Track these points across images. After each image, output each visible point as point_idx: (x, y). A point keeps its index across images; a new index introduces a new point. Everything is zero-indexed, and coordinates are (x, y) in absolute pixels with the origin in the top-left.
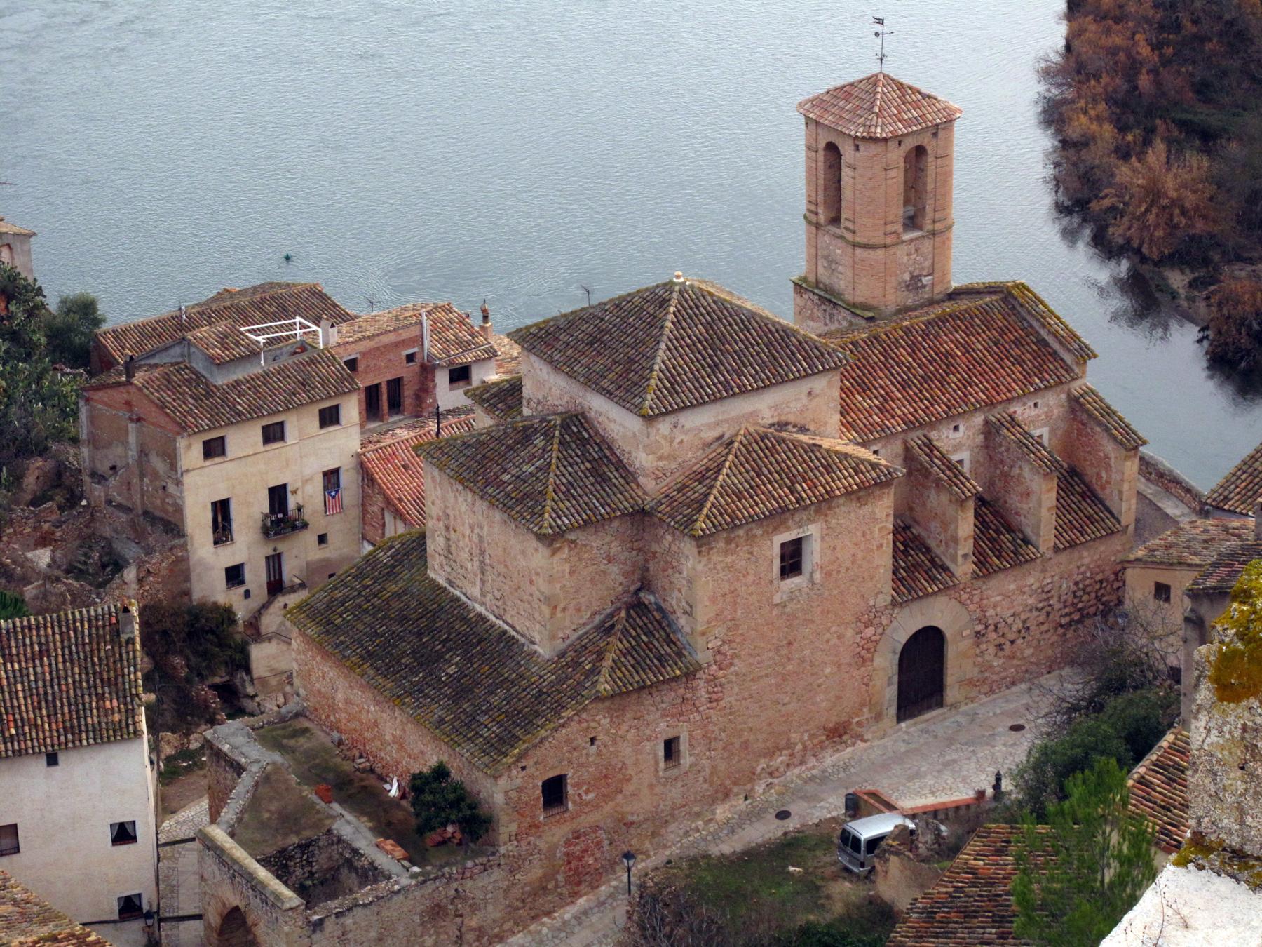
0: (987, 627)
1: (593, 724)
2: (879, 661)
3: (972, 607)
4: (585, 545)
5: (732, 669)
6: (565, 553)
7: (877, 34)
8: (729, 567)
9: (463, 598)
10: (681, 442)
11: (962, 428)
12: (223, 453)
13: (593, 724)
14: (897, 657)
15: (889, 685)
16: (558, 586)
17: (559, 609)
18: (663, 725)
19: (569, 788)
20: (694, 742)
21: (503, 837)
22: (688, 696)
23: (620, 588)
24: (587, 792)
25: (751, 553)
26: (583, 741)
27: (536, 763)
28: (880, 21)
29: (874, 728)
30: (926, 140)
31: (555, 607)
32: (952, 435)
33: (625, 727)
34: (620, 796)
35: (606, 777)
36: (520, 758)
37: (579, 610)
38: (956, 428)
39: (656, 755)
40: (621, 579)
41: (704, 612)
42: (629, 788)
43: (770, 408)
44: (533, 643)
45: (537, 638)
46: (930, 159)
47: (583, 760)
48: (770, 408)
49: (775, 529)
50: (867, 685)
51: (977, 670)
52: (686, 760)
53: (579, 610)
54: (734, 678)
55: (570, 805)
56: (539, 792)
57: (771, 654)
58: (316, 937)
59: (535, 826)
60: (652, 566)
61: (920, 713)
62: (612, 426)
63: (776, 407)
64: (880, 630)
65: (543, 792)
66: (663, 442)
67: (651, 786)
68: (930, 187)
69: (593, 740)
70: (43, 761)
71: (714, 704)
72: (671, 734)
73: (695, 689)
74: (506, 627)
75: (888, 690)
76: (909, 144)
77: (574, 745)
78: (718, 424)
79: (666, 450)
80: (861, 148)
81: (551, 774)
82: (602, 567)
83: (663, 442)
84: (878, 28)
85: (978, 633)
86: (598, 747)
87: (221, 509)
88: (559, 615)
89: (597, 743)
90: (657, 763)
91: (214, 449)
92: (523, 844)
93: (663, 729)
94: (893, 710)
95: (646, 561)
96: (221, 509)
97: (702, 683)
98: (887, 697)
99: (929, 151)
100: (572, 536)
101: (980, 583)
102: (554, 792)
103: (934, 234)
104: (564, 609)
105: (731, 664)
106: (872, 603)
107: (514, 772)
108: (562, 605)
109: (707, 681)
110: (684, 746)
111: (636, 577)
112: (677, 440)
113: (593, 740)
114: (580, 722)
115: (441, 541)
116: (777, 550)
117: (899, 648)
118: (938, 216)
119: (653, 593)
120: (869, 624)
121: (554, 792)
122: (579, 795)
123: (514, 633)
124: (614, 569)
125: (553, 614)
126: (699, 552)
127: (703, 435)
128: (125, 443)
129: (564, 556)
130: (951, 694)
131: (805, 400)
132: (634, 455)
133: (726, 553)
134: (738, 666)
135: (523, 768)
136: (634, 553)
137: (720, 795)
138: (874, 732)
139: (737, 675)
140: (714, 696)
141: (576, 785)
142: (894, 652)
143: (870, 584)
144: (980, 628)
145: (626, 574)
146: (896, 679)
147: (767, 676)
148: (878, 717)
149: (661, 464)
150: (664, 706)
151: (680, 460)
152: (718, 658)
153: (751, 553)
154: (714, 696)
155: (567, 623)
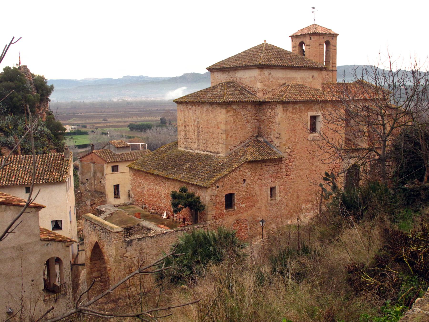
1: (245, 174)
4: (239, 112)
5: (294, 163)
6: (231, 113)
7: (313, 12)
8: (293, 119)
9: (191, 151)
10: (272, 81)
12: (118, 171)
13: (245, 174)
16: (229, 126)
17: (229, 137)
18: (270, 180)
19: (235, 200)
20: (281, 191)
21: (209, 217)
22: (279, 170)
23: (251, 134)
24: (242, 203)
25: (301, 116)
26: (240, 180)
27: (223, 186)
28: (314, 8)
30: (330, 39)
31: (228, 135)
33: (256, 178)
34: (254, 208)
35: (249, 198)
36: (217, 181)
37: (236, 139)
39: (267, 194)
40: (251, 130)
41: (285, 137)
42: (258, 205)
43: (300, 78)
44: (218, 153)
45: (220, 150)
46: (331, 46)
47: (241, 189)
48: (300, 78)
49: (309, 109)
52: (278, 198)
53: (236, 139)
54: (294, 167)
55: (236, 208)
56: (224, 199)
57: (307, 161)
58: (129, 248)
59: (222, 214)
60: (262, 126)
62: (246, 80)
63: (302, 78)
65: (225, 199)
66: (266, 79)
67: (265, 206)
68: (331, 55)
69: (244, 181)
70: (24, 191)
71: (288, 176)
72: (273, 185)
73: (281, 168)
74: (207, 153)
76: (326, 39)
77: (238, 181)
78: (284, 78)
79: (266, 83)
80: (312, 38)
81: (228, 192)
82: (245, 123)
83: (266, 79)
84: (313, 10)
86: (247, 184)
87: (117, 187)
88: (229, 139)
89: (246, 182)
90: (268, 197)
91: (115, 169)
92: (217, 221)
93: (270, 183)
95: (260, 125)
96: (117, 187)
97: (284, 166)
99: (331, 43)
100: (234, 107)
102: (229, 200)
103: (332, 71)
104: (231, 137)
105: (294, 161)
107: (214, 188)
108: (230, 135)
109: (286, 166)
110: (277, 191)
111: (257, 131)
112: (271, 80)
113: (244, 181)
114: (240, 171)
115: (183, 133)
116: (309, 118)
118: (334, 65)
119: (263, 137)
121: (229, 200)
122: (239, 204)
123: (211, 154)
124: (249, 125)
125: (227, 138)
126: (283, 110)
127: (279, 81)
128: (90, 172)
129: (231, 114)
131: (311, 79)
132: (255, 86)
133: (293, 113)
134: (296, 162)
135: (218, 187)
136: (256, 121)
137: (289, 216)
139: (296, 166)
140: (288, 173)
141: (238, 199)
145: (252, 128)
147: (305, 169)
149: (265, 88)
150: (271, 172)
151: (271, 89)
152: (289, 157)
153: (301, 116)
154: (288, 173)
155: (232, 143)
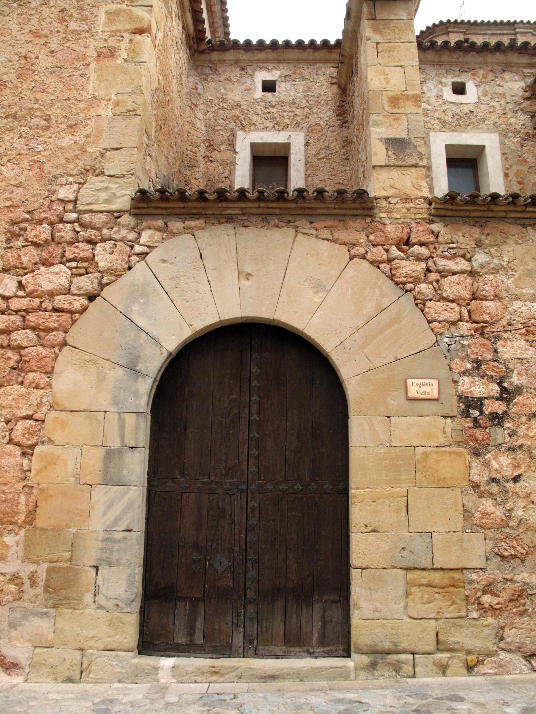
0: (507, 395)
2: (71, 379)
3: (435, 308)
11: (470, 87)
14: (145, 387)
15: (108, 480)
29: (42, 626)
32: (448, 94)
38: (459, 89)
50: (27, 451)
51: (475, 550)
61: (253, 648)
64: (87, 283)
75: (100, 495)
85: (470, 404)
94: (123, 582)
98: (98, 524)
101: (463, 237)
106: (65, 193)
117: (154, 363)
120: (49, 251)
130: (375, 605)
138: (40, 644)
142: (133, 370)
143: (67, 141)
144: (478, 388)
146: (137, 465)
148: (60, 589)
